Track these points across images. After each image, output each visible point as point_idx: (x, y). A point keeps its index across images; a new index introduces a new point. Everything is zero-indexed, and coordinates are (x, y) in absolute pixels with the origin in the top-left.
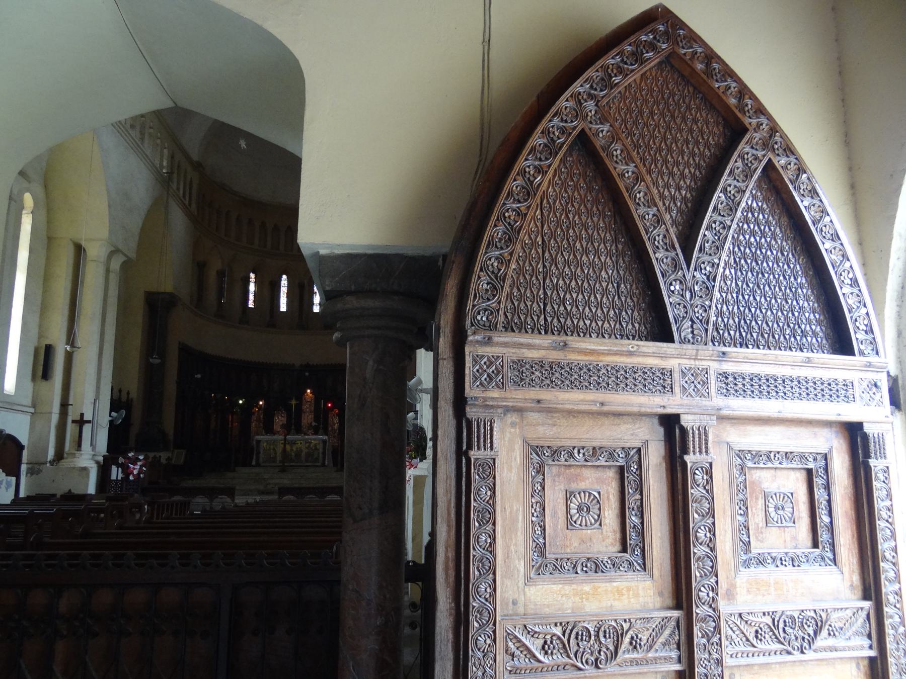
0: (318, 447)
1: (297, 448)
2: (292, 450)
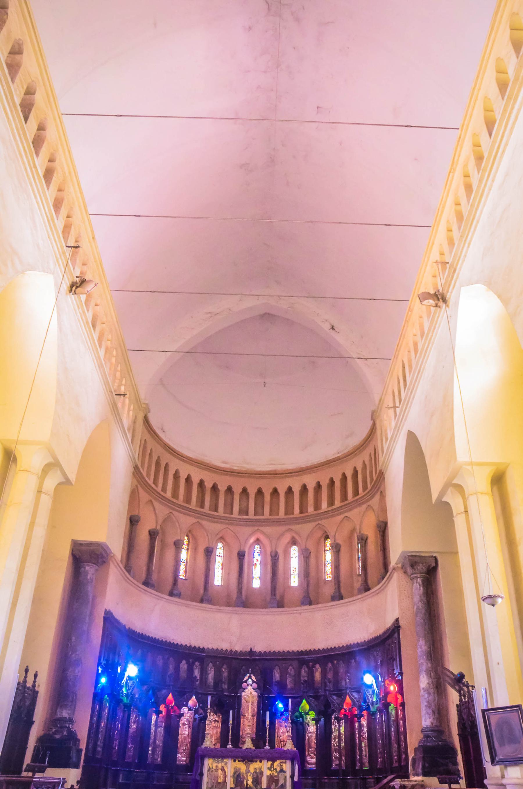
0: (285, 769)
1: (256, 769)
2: (248, 771)
